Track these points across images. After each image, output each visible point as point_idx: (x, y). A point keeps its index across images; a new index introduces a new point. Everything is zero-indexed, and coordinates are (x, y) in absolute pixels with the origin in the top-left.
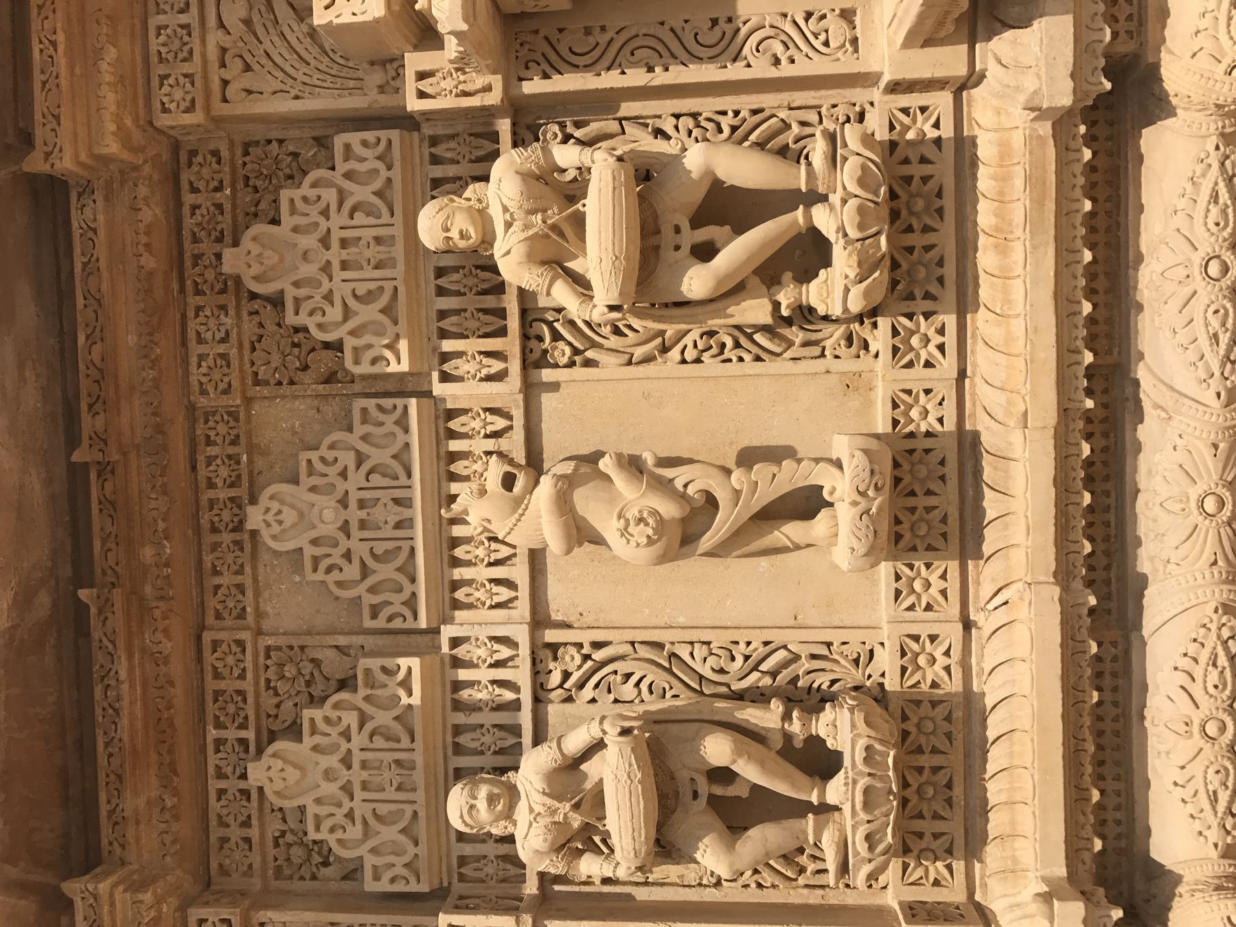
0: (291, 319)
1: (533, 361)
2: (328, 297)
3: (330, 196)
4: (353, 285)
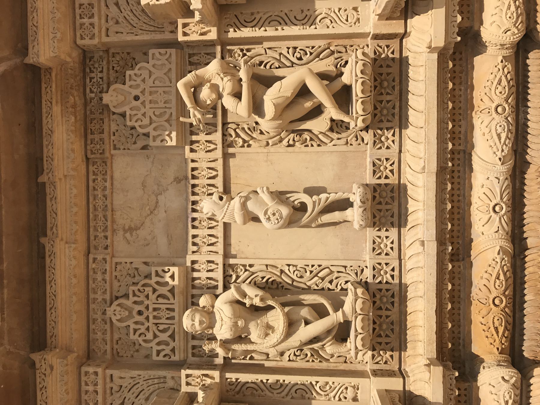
0: (129, 123)
1: (227, 144)
2: (144, 115)
3: (145, 74)
4: (153, 110)
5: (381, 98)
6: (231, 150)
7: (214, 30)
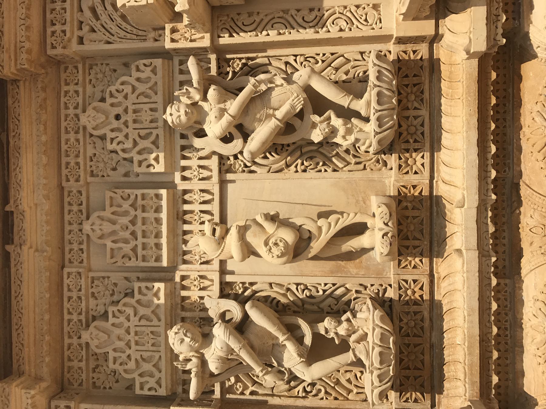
0: (110, 147)
2: (126, 136)
3: (128, 89)
4: (137, 131)
5: (406, 113)
6: (229, 176)
7: (208, 36)
